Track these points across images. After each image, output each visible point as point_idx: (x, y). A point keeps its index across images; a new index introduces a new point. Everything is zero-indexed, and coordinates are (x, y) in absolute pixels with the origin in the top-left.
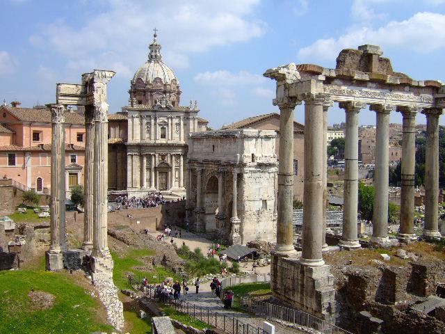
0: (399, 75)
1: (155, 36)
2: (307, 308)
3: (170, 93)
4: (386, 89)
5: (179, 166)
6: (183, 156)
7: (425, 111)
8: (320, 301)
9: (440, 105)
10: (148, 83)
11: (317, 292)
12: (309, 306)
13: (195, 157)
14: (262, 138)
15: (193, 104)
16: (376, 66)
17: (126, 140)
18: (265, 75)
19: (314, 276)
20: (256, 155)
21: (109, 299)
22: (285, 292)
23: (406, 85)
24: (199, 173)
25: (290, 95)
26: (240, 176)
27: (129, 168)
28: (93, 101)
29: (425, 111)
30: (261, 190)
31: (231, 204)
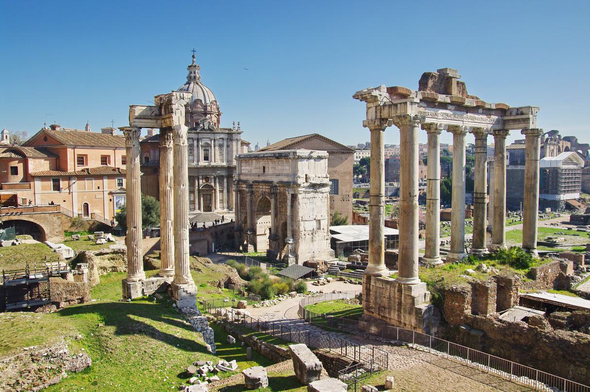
1: (193, 57)
2: (405, 325)
4: (463, 111)
6: (227, 179)
13: (243, 178)
15: (236, 126)
16: (455, 90)
18: (354, 97)
19: (413, 294)
20: (309, 175)
21: (200, 326)
22: (379, 309)
23: (480, 108)
25: (383, 117)
26: (294, 197)
30: (315, 210)
31: (285, 224)
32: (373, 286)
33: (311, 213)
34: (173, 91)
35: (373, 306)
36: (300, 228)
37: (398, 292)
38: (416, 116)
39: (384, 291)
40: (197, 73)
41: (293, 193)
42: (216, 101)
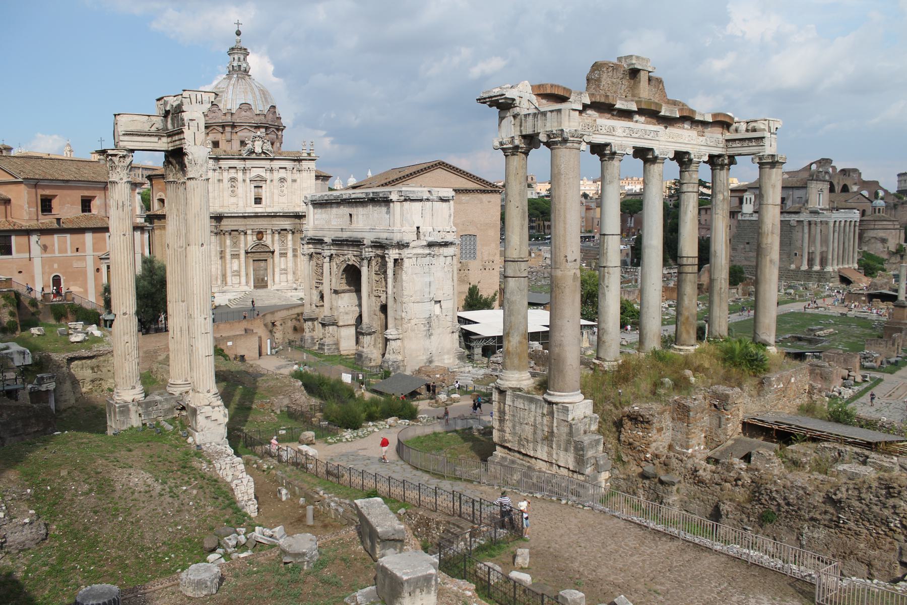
2: (559, 467)
5: (287, 249)
8: (583, 456)
11: (575, 442)
13: (319, 234)
16: (645, 91)
21: (230, 473)
24: (327, 259)
25: (524, 133)
32: (510, 406)
33: (427, 290)
35: (510, 438)
39: (526, 414)
41: (397, 257)
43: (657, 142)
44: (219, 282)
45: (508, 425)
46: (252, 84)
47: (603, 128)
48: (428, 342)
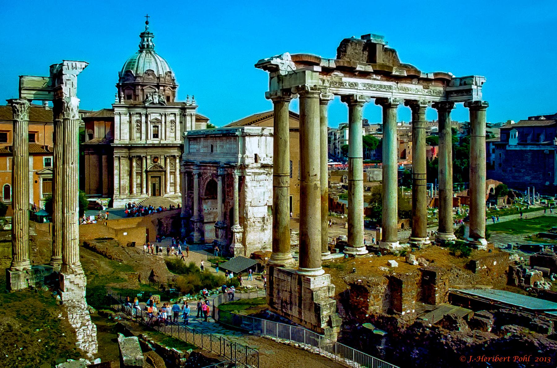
0: (405, 66)
2: (306, 322)
3: (142, 86)
4: (392, 81)
5: (175, 170)
7: (435, 105)
9: (451, 99)
10: (137, 76)
11: (315, 304)
12: (308, 321)
13: (192, 158)
14: (266, 136)
16: (380, 58)
17: (112, 141)
18: (256, 66)
19: (311, 288)
22: (282, 305)
24: (196, 176)
25: (284, 88)
26: (242, 179)
27: (116, 172)
28: (62, 96)
29: (435, 105)
31: (232, 210)
32: (276, 278)
33: (262, 198)
34: (64, 61)
35: (276, 301)
36: (249, 214)
37: (298, 284)
38: (315, 86)
39: (286, 283)
40: (149, 40)
42: (170, 72)
43: (391, 93)
44: (127, 192)
45: (275, 291)
46: (156, 57)
47: (347, 84)
48: (262, 234)
